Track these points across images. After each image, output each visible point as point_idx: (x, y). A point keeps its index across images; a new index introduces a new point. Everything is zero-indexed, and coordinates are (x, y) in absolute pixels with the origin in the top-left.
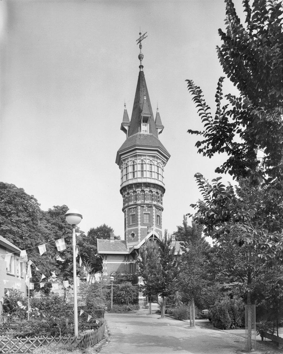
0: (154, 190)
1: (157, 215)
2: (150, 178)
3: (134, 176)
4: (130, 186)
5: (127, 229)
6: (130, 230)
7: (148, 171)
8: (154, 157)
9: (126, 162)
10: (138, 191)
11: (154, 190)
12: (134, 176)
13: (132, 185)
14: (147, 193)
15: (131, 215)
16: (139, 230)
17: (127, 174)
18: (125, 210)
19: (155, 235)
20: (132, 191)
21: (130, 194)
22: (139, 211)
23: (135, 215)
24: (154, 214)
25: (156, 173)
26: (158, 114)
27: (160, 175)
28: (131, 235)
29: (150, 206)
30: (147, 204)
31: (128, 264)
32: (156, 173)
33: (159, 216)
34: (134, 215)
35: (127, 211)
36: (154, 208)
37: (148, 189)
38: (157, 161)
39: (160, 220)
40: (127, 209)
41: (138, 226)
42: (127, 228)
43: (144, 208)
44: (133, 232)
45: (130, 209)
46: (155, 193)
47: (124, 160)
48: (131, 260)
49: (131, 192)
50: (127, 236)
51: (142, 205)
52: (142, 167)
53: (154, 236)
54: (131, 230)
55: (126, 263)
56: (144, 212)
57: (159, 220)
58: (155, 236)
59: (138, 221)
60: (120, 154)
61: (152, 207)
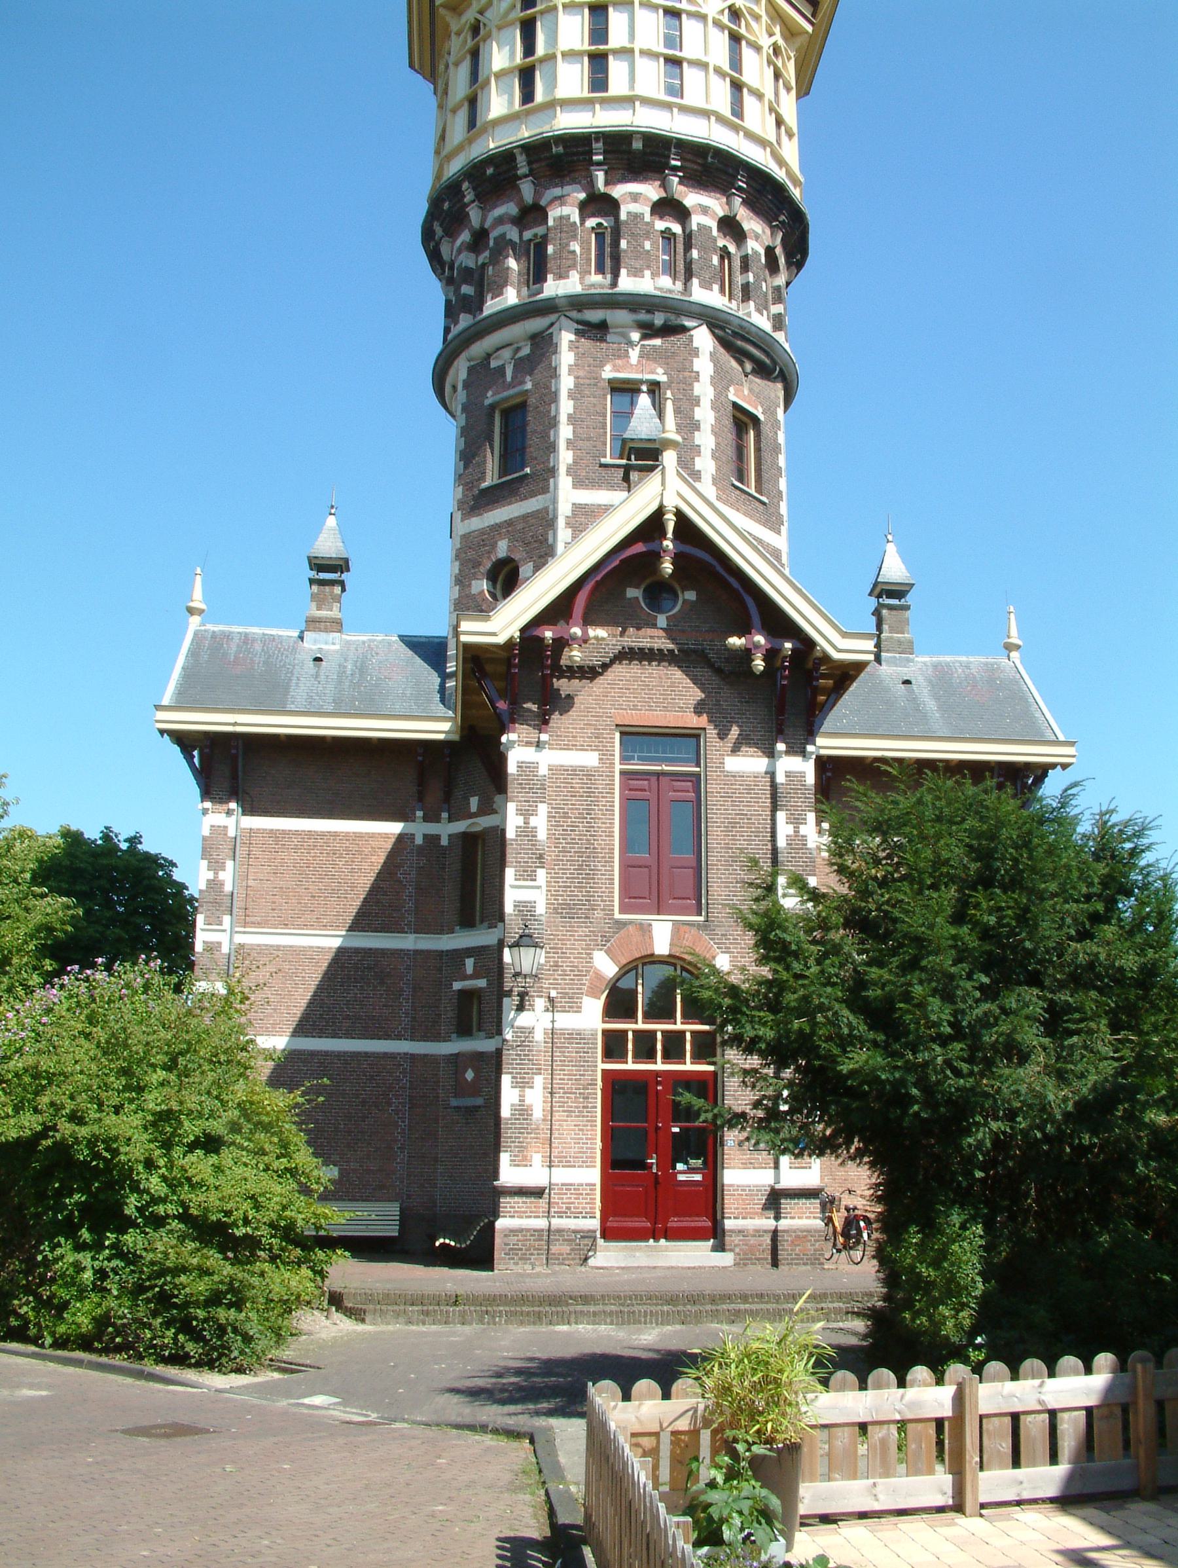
1: (735, 406)
2: (668, 106)
3: (528, 95)
4: (494, 176)
6: (482, 532)
7: (643, 53)
9: (470, 15)
12: (528, 95)
13: (505, 159)
14: (636, 217)
15: (493, 407)
16: (561, 522)
18: (452, 372)
19: (679, 514)
20: (509, 208)
21: (493, 235)
22: (566, 357)
23: (532, 401)
24: (704, 390)
25: (719, 71)
27: (759, 96)
28: (492, 576)
29: (663, 321)
30: (635, 303)
31: (444, 842)
32: (719, 71)
33: (755, 420)
36: (702, 338)
37: (651, 191)
39: (765, 455)
40: (460, 370)
41: (545, 490)
44: (502, 549)
45: (488, 356)
46: (714, 225)
48: (474, 802)
49: (500, 221)
51: (594, 316)
52: (599, 33)
53: (670, 527)
55: (432, 828)
56: (608, 373)
57: (758, 450)
58: (687, 529)
59: (552, 448)
61: (684, 329)
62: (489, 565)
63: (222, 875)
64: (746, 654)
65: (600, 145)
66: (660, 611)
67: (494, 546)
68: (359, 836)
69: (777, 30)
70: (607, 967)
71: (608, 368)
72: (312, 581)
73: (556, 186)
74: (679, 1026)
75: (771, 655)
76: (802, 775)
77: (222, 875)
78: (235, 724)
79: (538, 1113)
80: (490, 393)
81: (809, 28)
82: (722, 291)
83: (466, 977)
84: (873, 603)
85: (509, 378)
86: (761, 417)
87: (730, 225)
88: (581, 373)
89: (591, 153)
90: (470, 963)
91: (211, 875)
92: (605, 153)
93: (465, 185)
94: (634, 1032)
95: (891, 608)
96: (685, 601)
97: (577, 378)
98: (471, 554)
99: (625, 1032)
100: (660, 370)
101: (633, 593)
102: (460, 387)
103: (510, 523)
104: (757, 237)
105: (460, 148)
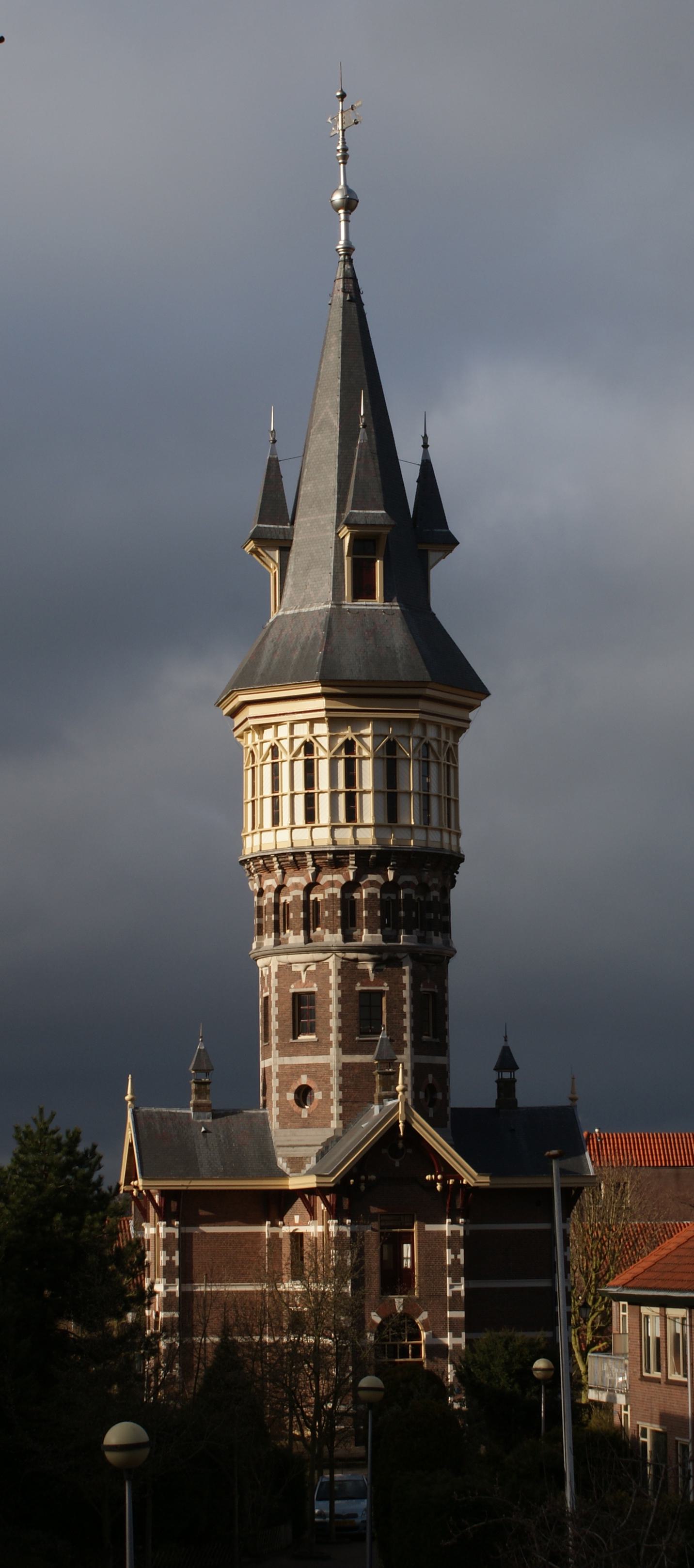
6: (292, 1067)
10: (332, 884)
11: (409, 878)
23: (319, 999)
44: (304, 1080)
54: (298, 1070)
56: (359, 987)
62: (296, 1088)
63: (173, 1258)
64: (433, 1182)
67: (299, 1077)
68: (238, 1234)
71: (358, 984)
73: (329, 874)
75: (443, 1182)
76: (459, 1232)
77: (173, 1258)
80: (292, 986)
88: (344, 989)
91: (168, 1258)
94: (388, 1345)
97: (342, 991)
100: (386, 984)
101: (385, 1151)
102: (273, 976)
103: (308, 1065)
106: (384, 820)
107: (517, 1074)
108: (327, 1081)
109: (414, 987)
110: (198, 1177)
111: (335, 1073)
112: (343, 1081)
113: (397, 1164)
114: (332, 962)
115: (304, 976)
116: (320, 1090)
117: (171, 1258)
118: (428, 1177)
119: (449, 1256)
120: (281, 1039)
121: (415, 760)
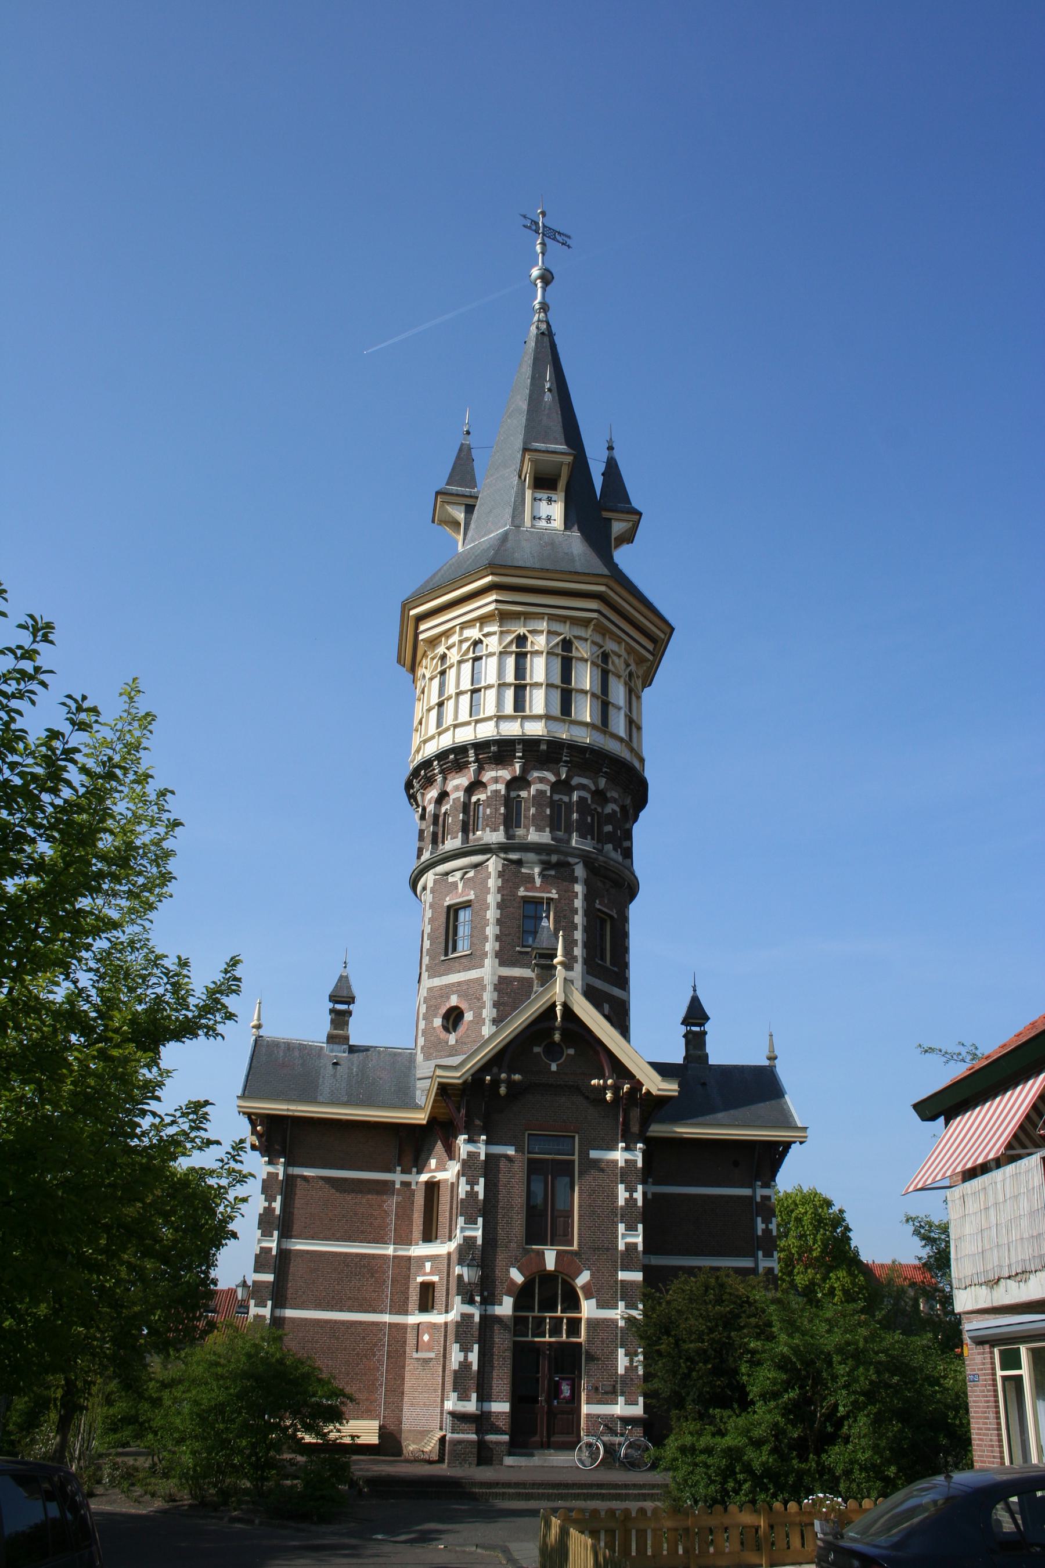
0: (584, 781)
2: (564, 721)
5: (427, 983)
6: (441, 988)
8: (585, 623)
9: (441, 650)
10: (496, 780)
11: (584, 781)
13: (460, 750)
17: (440, 705)
18: (423, 880)
23: (475, 905)
26: (612, 469)
33: (611, 917)
34: (467, 905)
35: (430, 885)
36: (580, 871)
38: (601, 647)
42: (425, 975)
43: (524, 870)
44: (454, 1001)
45: (447, 874)
47: (433, 642)
50: (422, 1024)
51: (514, 856)
54: (445, 991)
56: (522, 892)
60: (412, 613)
61: (569, 865)
65: (520, 747)
66: (554, 1061)
67: (448, 998)
69: (631, 662)
70: (517, 1276)
71: (522, 889)
72: (332, 1011)
74: (559, 1314)
75: (616, 1089)
77: (274, 1205)
78: (288, 1110)
79: (475, 1367)
80: (448, 899)
81: (651, 658)
82: (593, 839)
83: (425, 1274)
84: (683, 1029)
85: (460, 890)
86: (615, 916)
87: (600, 795)
88: (505, 892)
89: (515, 751)
90: (428, 1265)
92: (523, 751)
93: (435, 763)
94: (533, 1317)
95: (695, 1033)
96: (568, 1055)
98: (433, 1002)
99: (528, 1317)
100: (554, 891)
101: (537, 1049)
104: (615, 801)
105: (432, 738)
106: (556, 711)
107: (708, 1027)
108: (479, 998)
109: (588, 898)
110: (313, 1101)
111: (490, 988)
112: (498, 997)
113: (554, 1067)
114: (493, 864)
115: (460, 886)
116: (471, 1009)
117: (270, 1204)
118: (594, 1082)
119: (622, 1194)
120: (432, 958)
121: (593, 663)
